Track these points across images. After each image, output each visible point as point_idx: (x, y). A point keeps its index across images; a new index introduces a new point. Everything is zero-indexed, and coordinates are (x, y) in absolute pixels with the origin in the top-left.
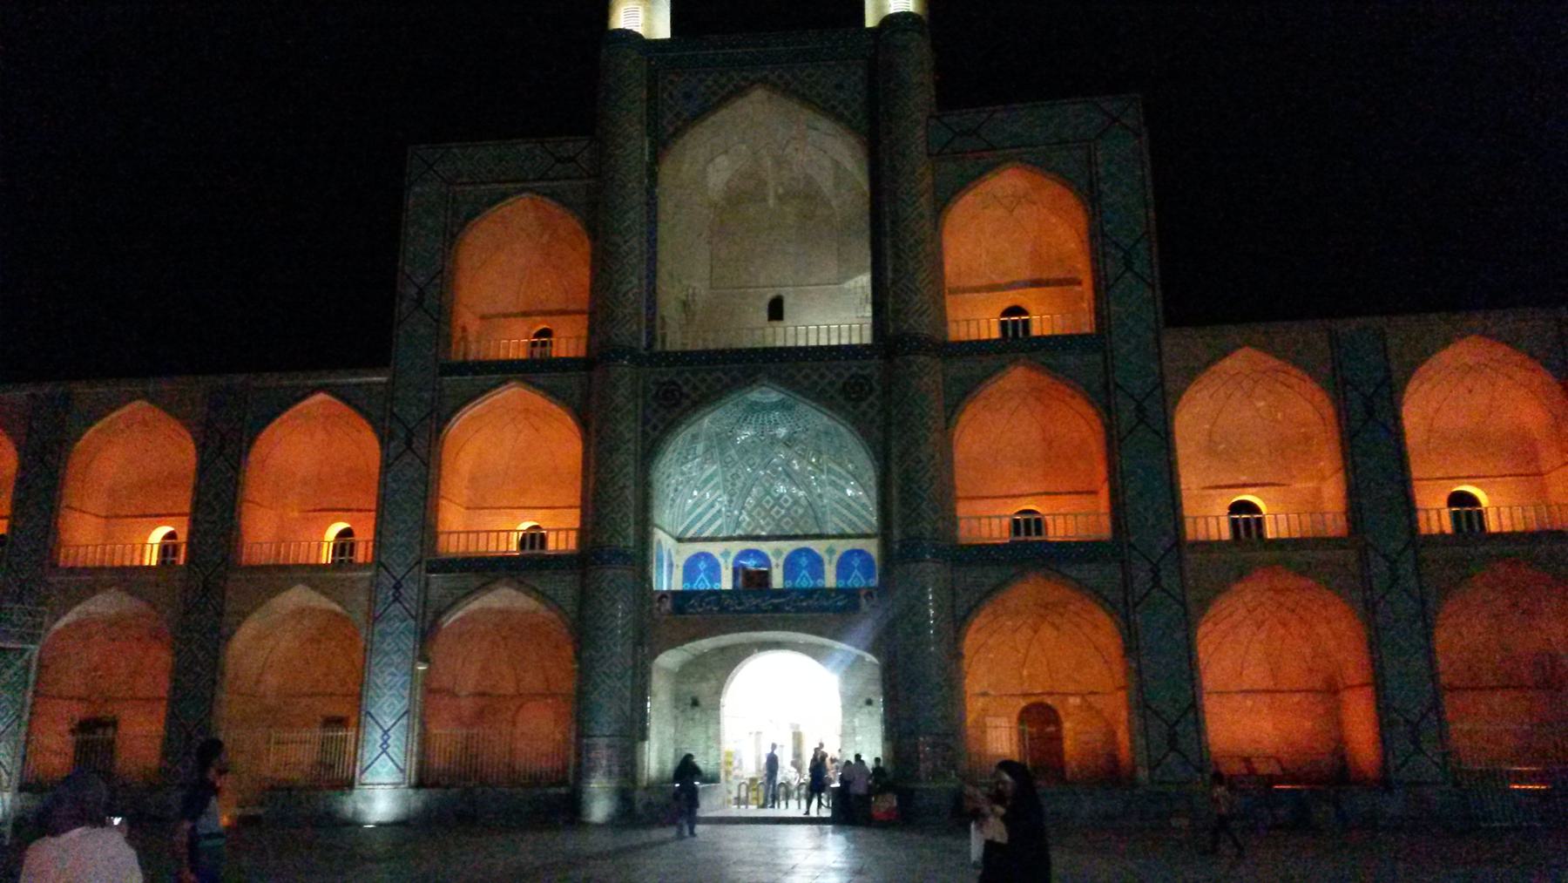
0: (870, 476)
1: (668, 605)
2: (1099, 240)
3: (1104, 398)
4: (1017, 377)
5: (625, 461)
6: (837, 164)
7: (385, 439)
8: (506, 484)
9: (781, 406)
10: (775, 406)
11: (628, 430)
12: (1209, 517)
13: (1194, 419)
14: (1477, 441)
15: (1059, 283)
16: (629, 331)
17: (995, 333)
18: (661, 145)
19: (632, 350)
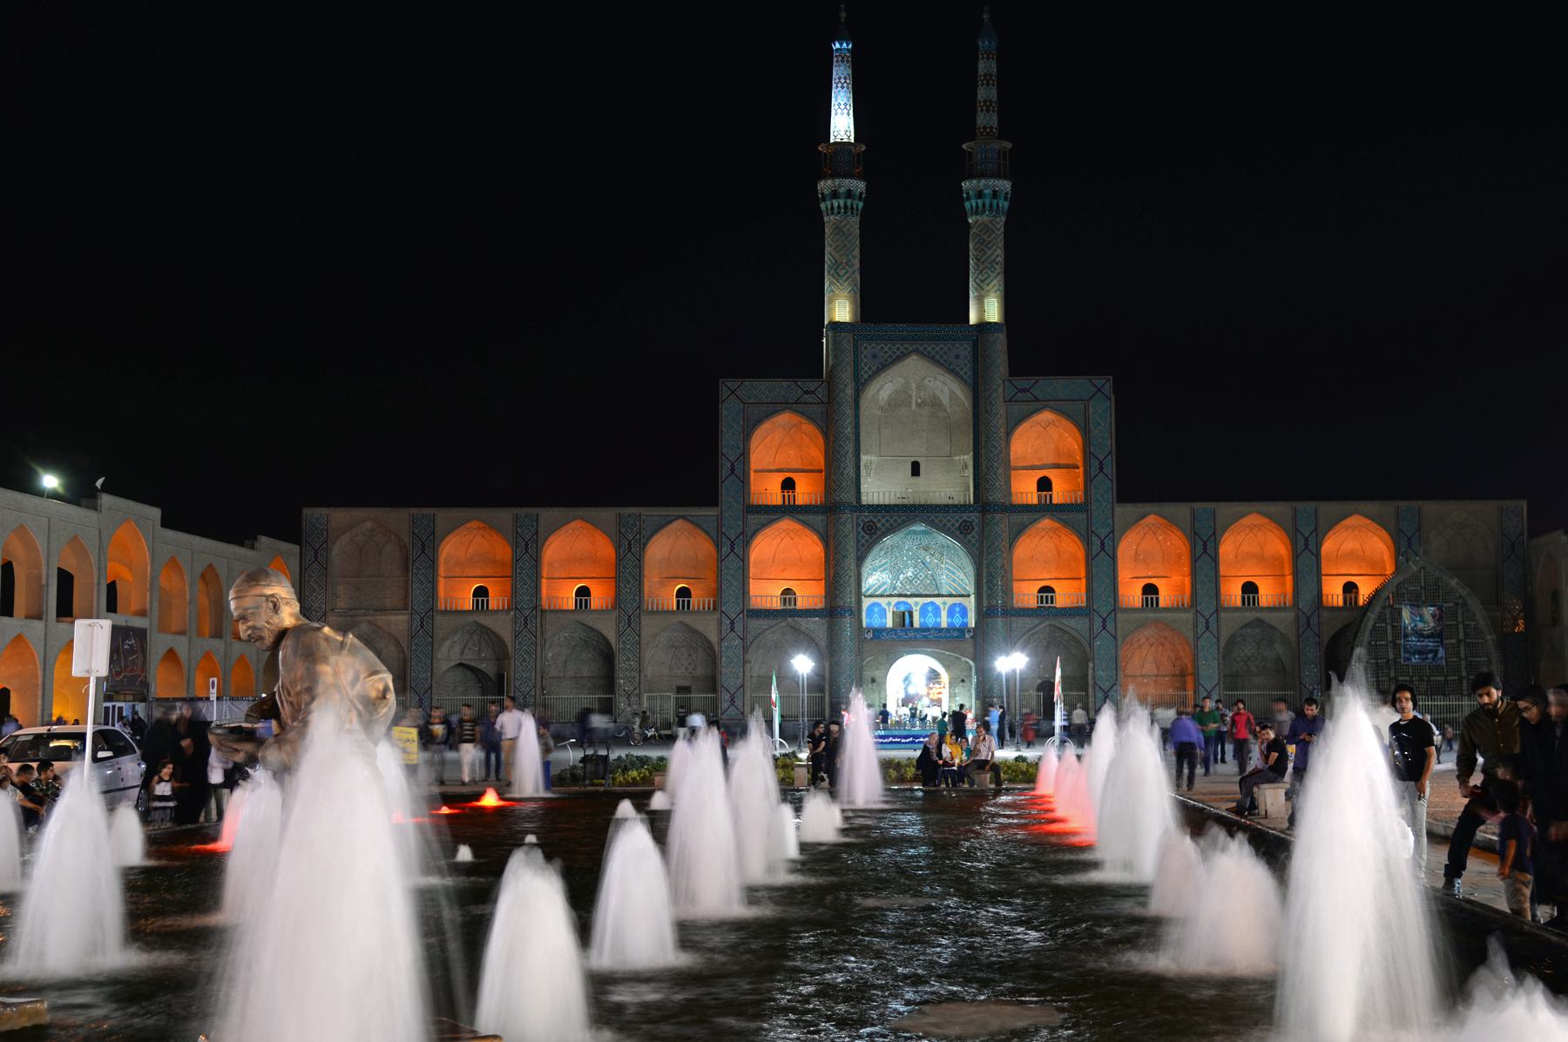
0: (970, 569)
1: (870, 635)
2: (1088, 453)
3: (1086, 538)
4: (1046, 523)
5: (851, 560)
6: (952, 393)
7: (718, 545)
8: (781, 567)
9: (925, 533)
10: (921, 532)
11: (851, 546)
12: (1132, 594)
13: (1127, 547)
14: (1260, 559)
15: (1068, 467)
16: (847, 496)
17: (1035, 501)
18: (860, 386)
19: (850, 505)
